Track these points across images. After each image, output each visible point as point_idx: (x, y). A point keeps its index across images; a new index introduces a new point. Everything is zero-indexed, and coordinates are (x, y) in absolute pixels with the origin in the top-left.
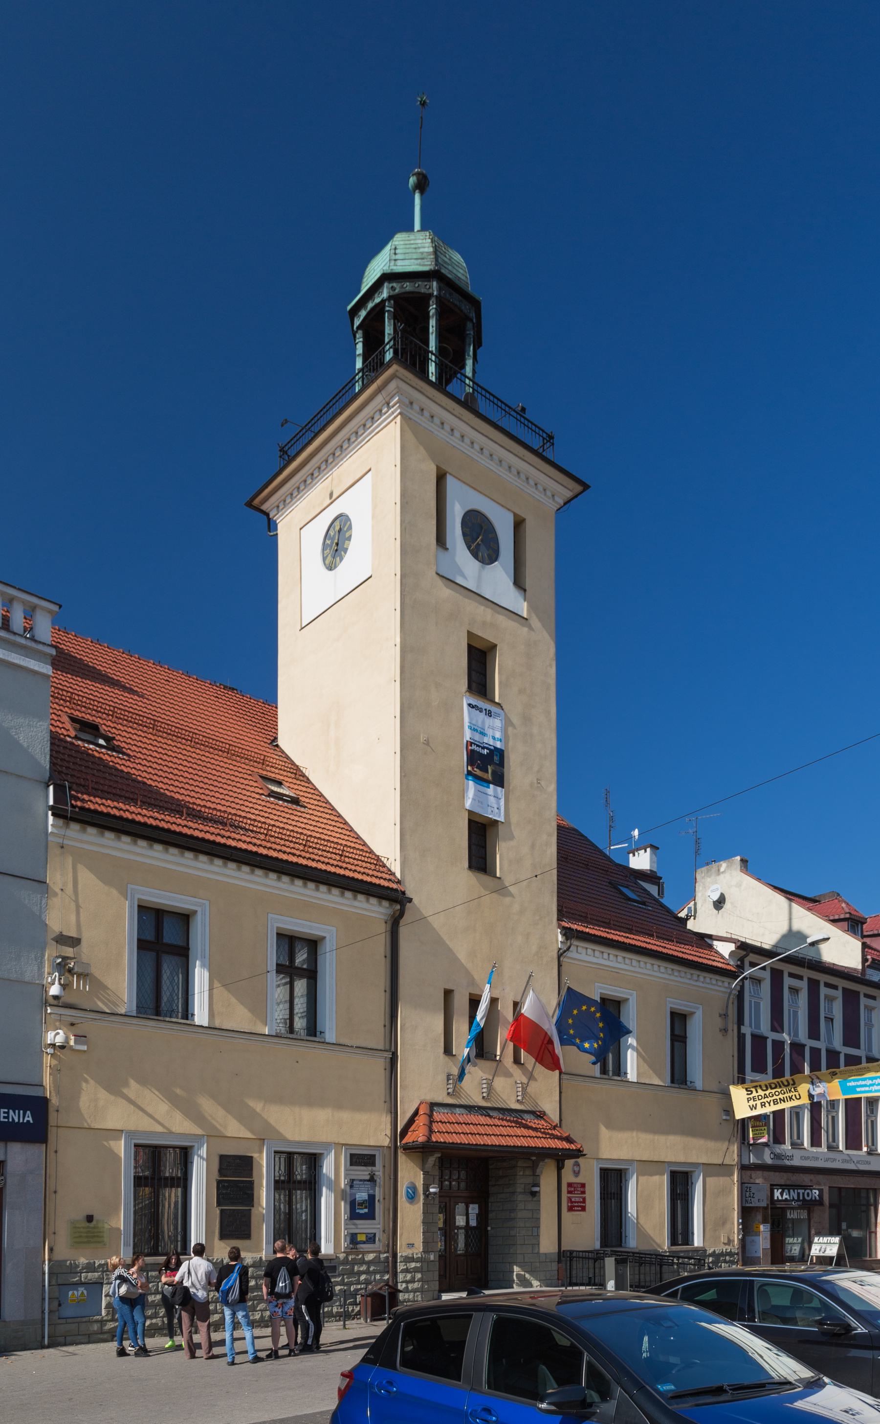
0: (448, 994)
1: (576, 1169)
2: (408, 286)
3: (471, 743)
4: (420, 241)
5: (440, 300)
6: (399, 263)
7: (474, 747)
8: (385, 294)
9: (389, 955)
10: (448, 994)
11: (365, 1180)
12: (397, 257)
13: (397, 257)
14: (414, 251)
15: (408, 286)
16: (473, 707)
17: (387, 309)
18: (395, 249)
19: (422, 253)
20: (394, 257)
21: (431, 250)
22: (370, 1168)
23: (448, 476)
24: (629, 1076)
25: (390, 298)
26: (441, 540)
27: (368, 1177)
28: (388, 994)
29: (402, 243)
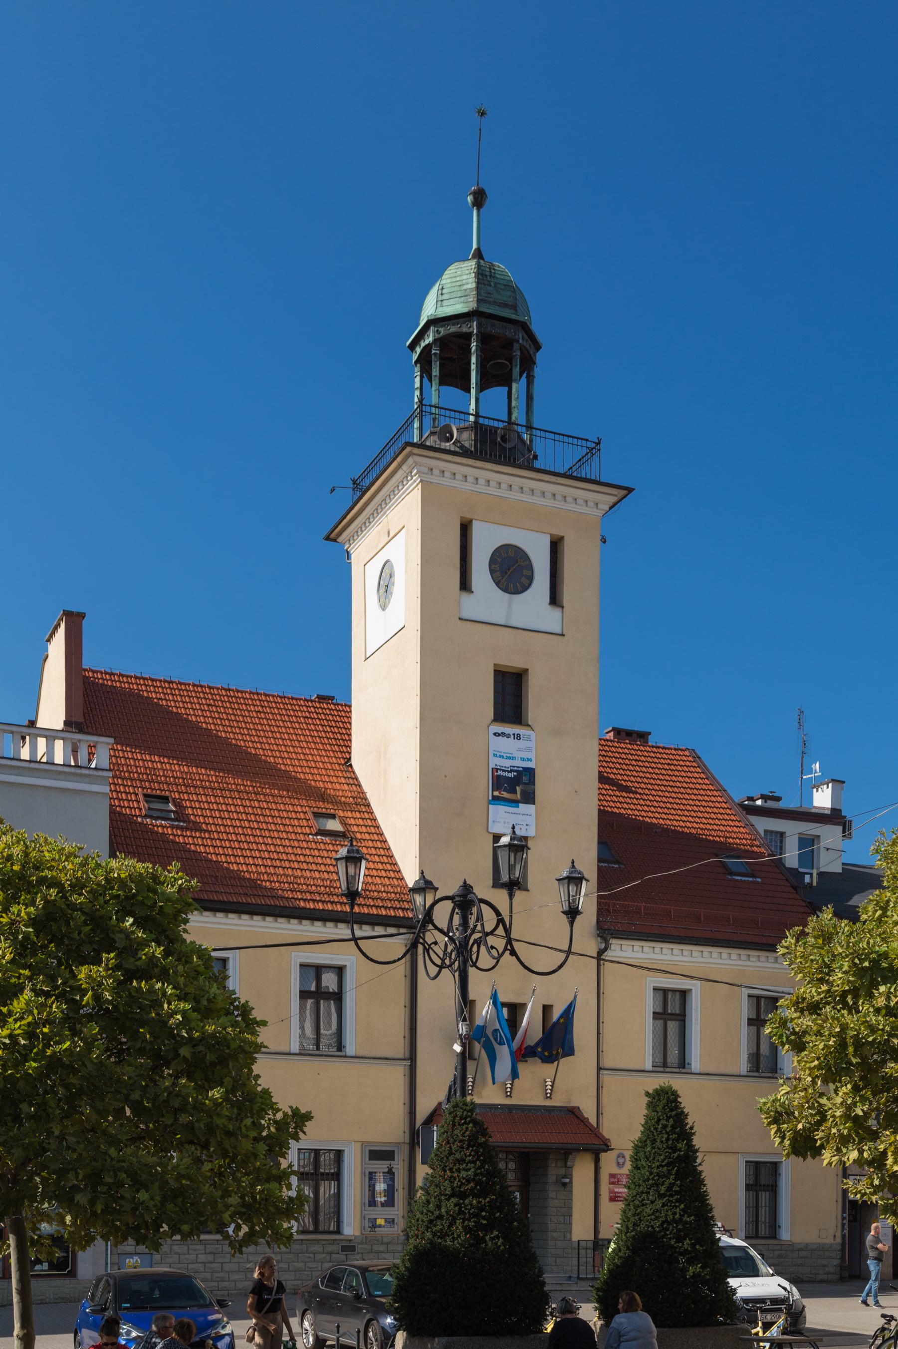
3: (497, 770)
4: (465, 277)
6: (445, 303)
7: (500, 772)
8: (429, 339)
9: (409, 975)
12: (445, 297)
13: (445, 297)
14: (458, 289)
16: (499, 735)
17: (433, 352)
18: (442, 289)
19: (465, 290)
20: (440, 298)
21: (474, 285)
22: (388, 1162)
23: (474, 522)
24: (693, 1067)
25: (435, 341)
26: (465, 585)
27: (386, 1170)
28: (408, 1010)
29: (449, 281)
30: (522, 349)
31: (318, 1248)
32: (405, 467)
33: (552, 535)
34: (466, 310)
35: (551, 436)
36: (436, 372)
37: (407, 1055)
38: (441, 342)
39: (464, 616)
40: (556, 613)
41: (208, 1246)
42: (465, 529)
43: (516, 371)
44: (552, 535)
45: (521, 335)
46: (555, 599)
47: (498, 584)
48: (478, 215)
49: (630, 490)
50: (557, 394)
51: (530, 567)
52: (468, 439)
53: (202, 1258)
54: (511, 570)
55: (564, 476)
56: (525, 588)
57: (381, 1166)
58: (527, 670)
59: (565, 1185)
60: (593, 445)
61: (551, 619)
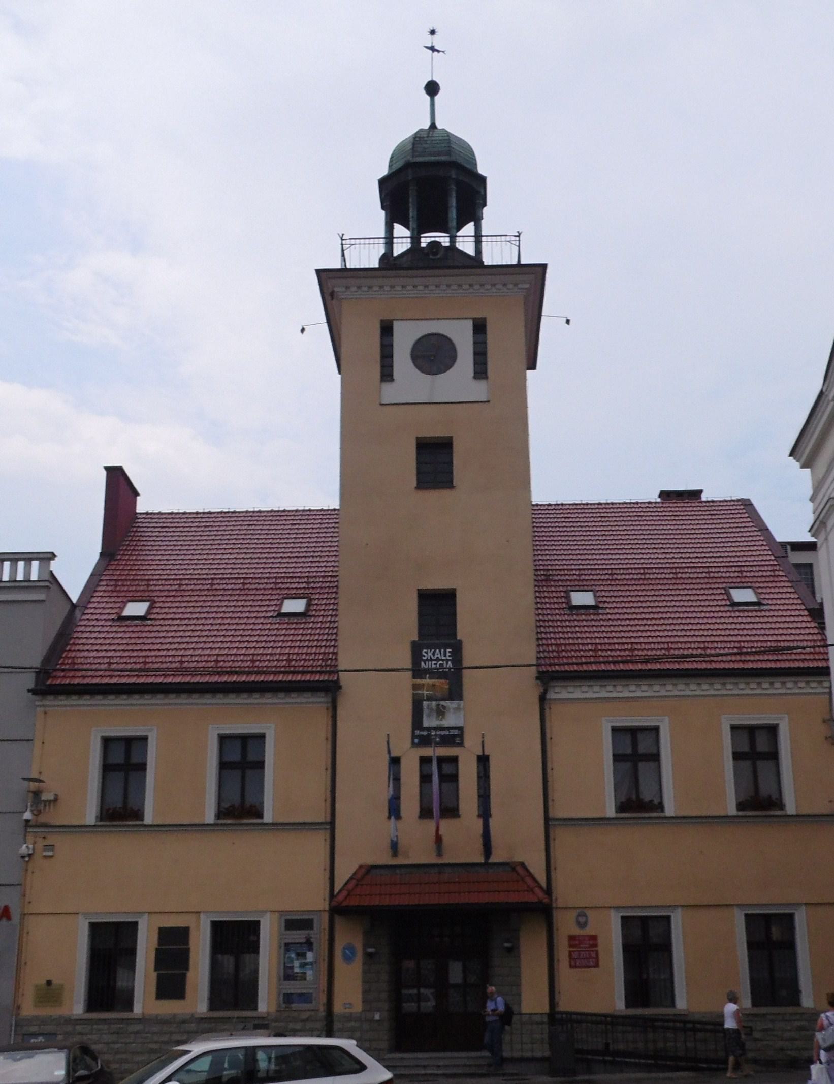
0: (395, 761)
1: (582, 920)
10: (395, 761)
11: (301, 943)
22: (307, 932)
30: (458, 183)
33: (474, 320)
37: (328, 820)
39: (385, 401)
40: (482, 385)
41: (112, 1026)
44: (474, 320)
45: (453, 174)
46: (481, 372)
53: (106, 1038)
54: (434, 355)
56: (448, 367)
57: (298, 936)
59: (513, 951)
61: (478, 390)
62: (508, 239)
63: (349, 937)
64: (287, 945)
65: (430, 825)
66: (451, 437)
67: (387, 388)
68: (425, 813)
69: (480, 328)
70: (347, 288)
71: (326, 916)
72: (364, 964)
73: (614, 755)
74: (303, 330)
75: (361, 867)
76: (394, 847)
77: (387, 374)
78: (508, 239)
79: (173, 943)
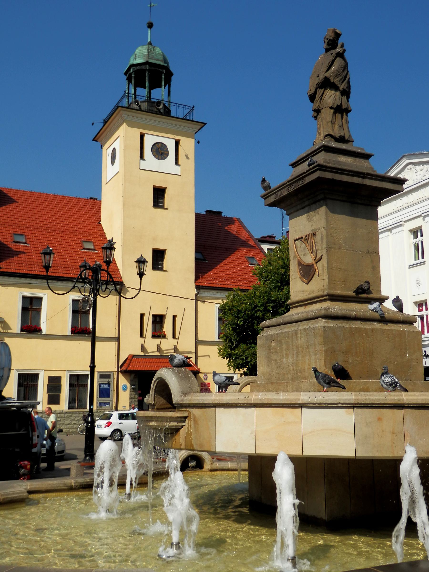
0: (142, 316)
2: (139, 67)
5: (149, 70)
8: (131, 71)
10: (142, 316)
11: (105, 384)
15: (139, 67)
22: (108, 379)
31: (77, 415)
32: (119, 115)
33: (176, 140)
34: (144, 62)
35: (176, 105)
36: (133, 81)
37: (117, 336)
38: (135, 72)
42: (142, 136)
43: (163, 83)
47: (155, 156)
48: (151, 31)
49: (205, 124)
50: (180, 92)
51: (167, 150)
52: (144, 106)
54: (160, 151)
55: (183, 119)
56: (165, 158)
57: (105, 381)
58: (166, 188)
60: (192, 108)
61: (177, 170)
62: (190, 108)
63: (123, 381)
64: (100, 384)
65: (157, 341)
66: (166, 188)
67: (142, 161)
68: (154, 336)
69: (177, 143)
70: (129, 116)
71: (115, 374)
72: (130, 392)
73: (218, 318)
74: (93, 124)
75: (129, 355)
76: (143, 348)
77: (142, 157)
78: (190, 108)
79: (54, 384)
